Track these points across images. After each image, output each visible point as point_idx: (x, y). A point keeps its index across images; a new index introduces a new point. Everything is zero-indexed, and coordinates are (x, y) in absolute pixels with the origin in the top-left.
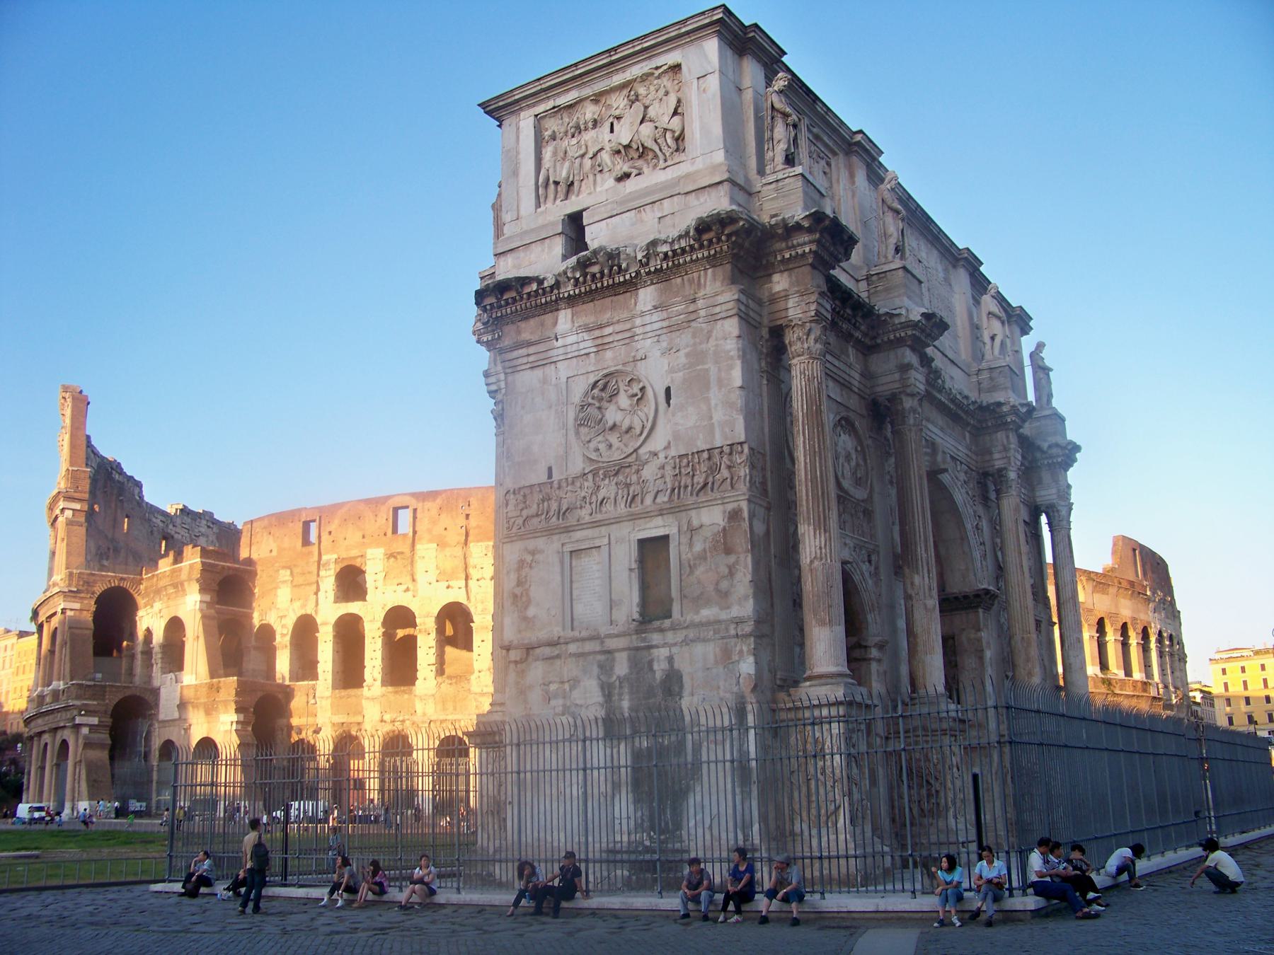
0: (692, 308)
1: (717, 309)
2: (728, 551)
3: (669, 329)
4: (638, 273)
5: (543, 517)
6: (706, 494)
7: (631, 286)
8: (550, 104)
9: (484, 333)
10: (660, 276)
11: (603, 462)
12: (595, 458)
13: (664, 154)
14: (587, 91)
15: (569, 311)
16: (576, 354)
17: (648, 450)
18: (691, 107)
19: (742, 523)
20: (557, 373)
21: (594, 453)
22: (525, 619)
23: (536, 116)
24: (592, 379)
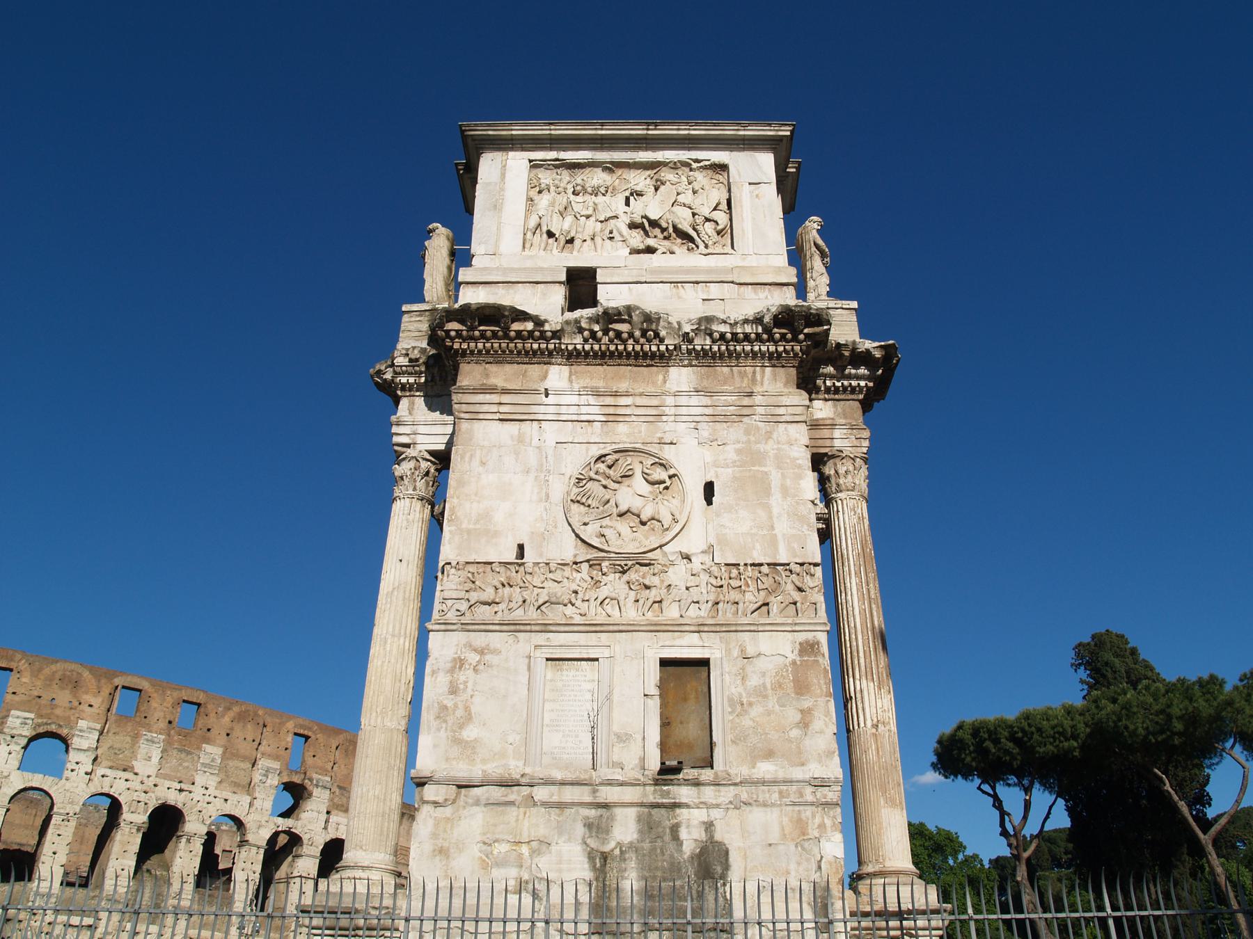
0: (746, 401)
1: (781, 411)
6: (761, 616)
7: (662, 359)
10: (705, 358)
11: (609, 552)
13: (703, 241)
15: (566, 369)
16: (575, 417)
17: (678, 550)
18: (741, 206)
19: (820, 659)
21: (598, 540)
22: (457, 741)
23: (530, 161)
24: (596, 451)
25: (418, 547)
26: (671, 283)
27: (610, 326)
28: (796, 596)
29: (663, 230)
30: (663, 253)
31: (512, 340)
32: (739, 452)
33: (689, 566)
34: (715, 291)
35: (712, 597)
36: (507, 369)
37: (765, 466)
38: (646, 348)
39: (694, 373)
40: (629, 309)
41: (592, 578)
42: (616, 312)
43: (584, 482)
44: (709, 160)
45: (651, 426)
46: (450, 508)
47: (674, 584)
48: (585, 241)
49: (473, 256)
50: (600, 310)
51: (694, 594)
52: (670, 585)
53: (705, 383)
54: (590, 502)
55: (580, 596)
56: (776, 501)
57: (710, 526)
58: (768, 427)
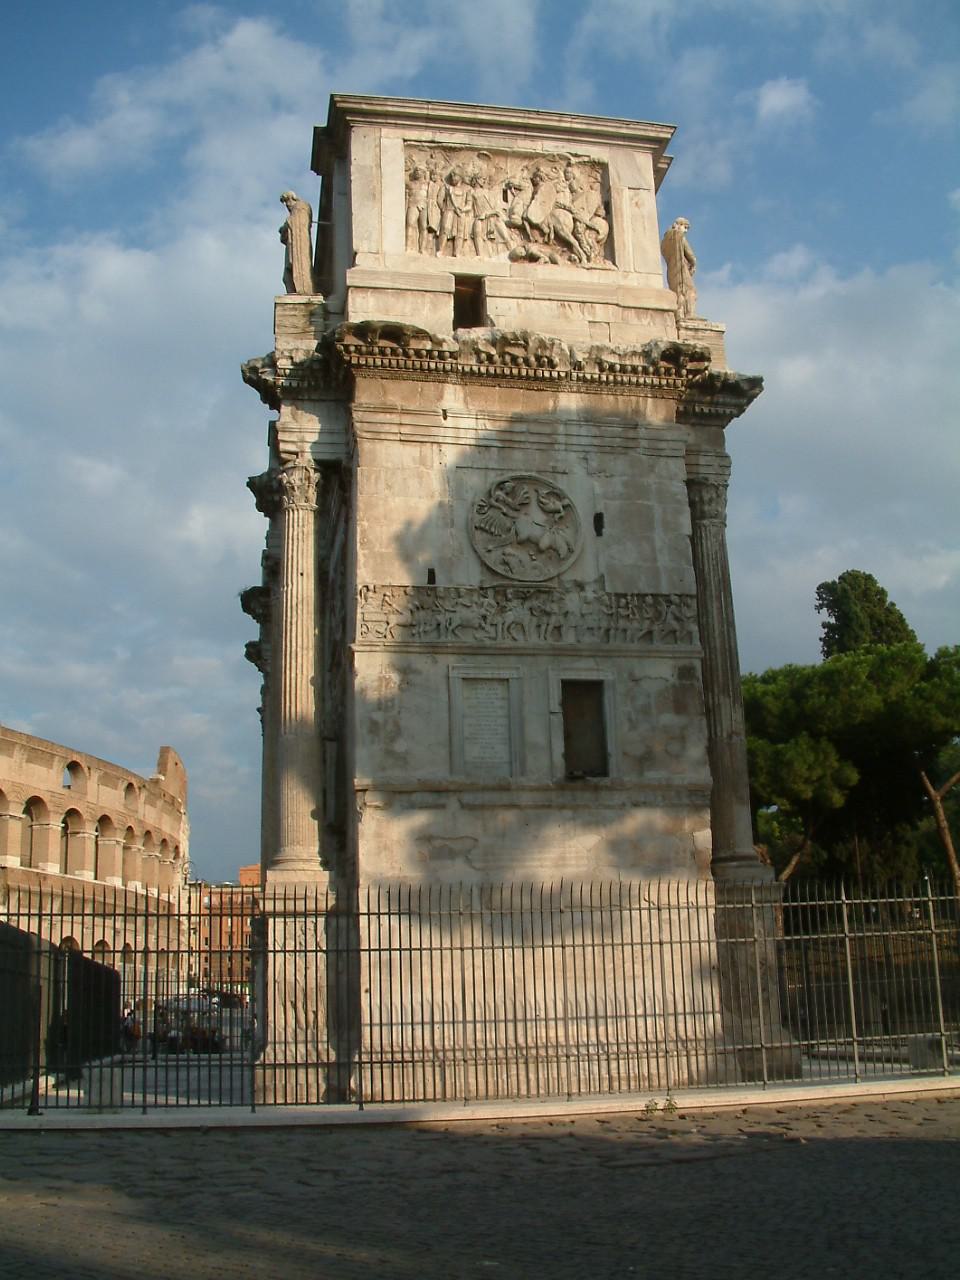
0: (631, 434)
1: (663, 445)
2: (679, 708)
4: (568, 375)
8: (427, 135)
11: (513, 579)
12: (504, 573)
14: (481, 142)
17: (573, 578)
18: (622, 216)
22: (390, 753)
28: (675, 625)
29: (543, 234)
30: (546, 263)
32: (625, 484)
33: (582, 594)
35: (604, 624)
37: (648, 500)
38: (540, 373)
44: (588, 156)
46: (362, 531)
47: (570, 610)
48: (466, 240)
49: (356, 253)
51: (590, 621)
52: (567, 612)
56: (659, 537)
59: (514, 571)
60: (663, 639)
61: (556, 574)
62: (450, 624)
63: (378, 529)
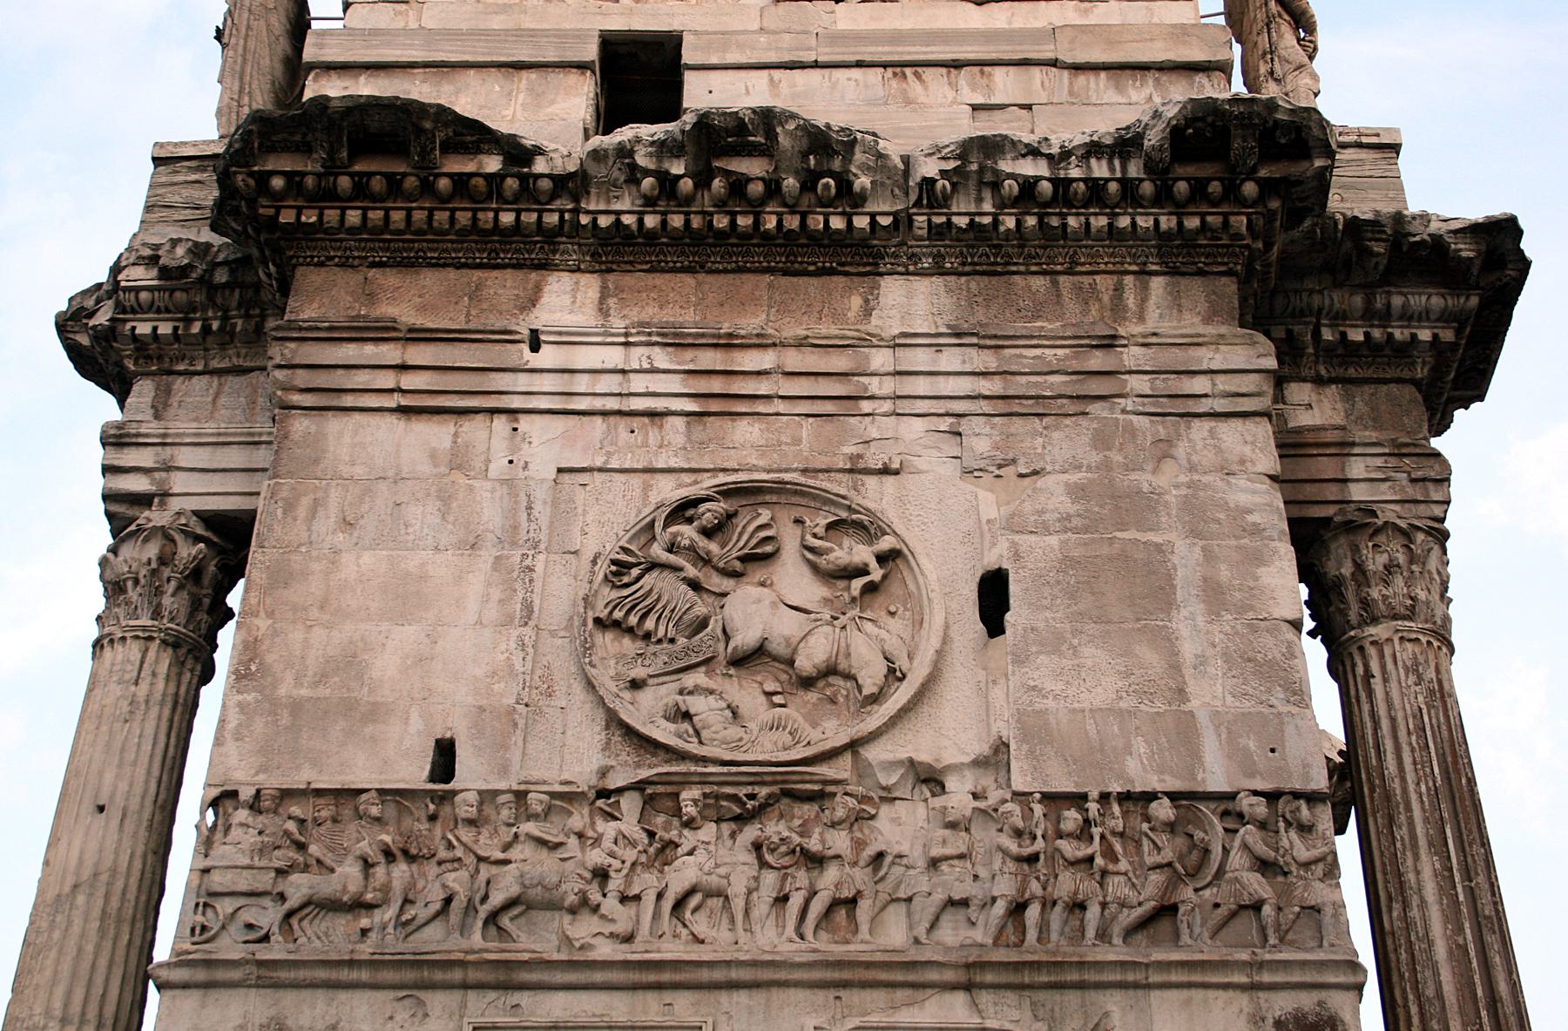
1: (1199, 385)
3: (1001, 407)
4: (902, 221)
5: (390, 913)
6: (1154, 942)
9: (151, 307)
11: (704, 760)
15: (590, 285)
16: (612, 404)
17: (903, 755)
20: (515, 449)
21: (672, 727)
24: (670, 491)
25: (156, 772)
26: (885, 65)
27: (717, 164)
28: (1257, 885)
31: (444, 200)
32: (1077, 492)
33: (937, 802)
34: (1005, 85)
35: (1005, 887)
36: (428, 282)
38: (816, 222)
39: (949, 291)
40: (768, 118)
41: (651, 835)
42: (732, 124)
43: (635, 572)
45: (829, 427)
50: (689, 119)
51: (954, 880)
52: (880, 856)
53: (980, 315)
54: (650, 624)
55: (615, 883)
57: (998, 693)
58: (1162, 429)
59: (705, 734)
60: (1214, 935)
61: (842, 739)
62: (485, 899)
63: (296, 636)
